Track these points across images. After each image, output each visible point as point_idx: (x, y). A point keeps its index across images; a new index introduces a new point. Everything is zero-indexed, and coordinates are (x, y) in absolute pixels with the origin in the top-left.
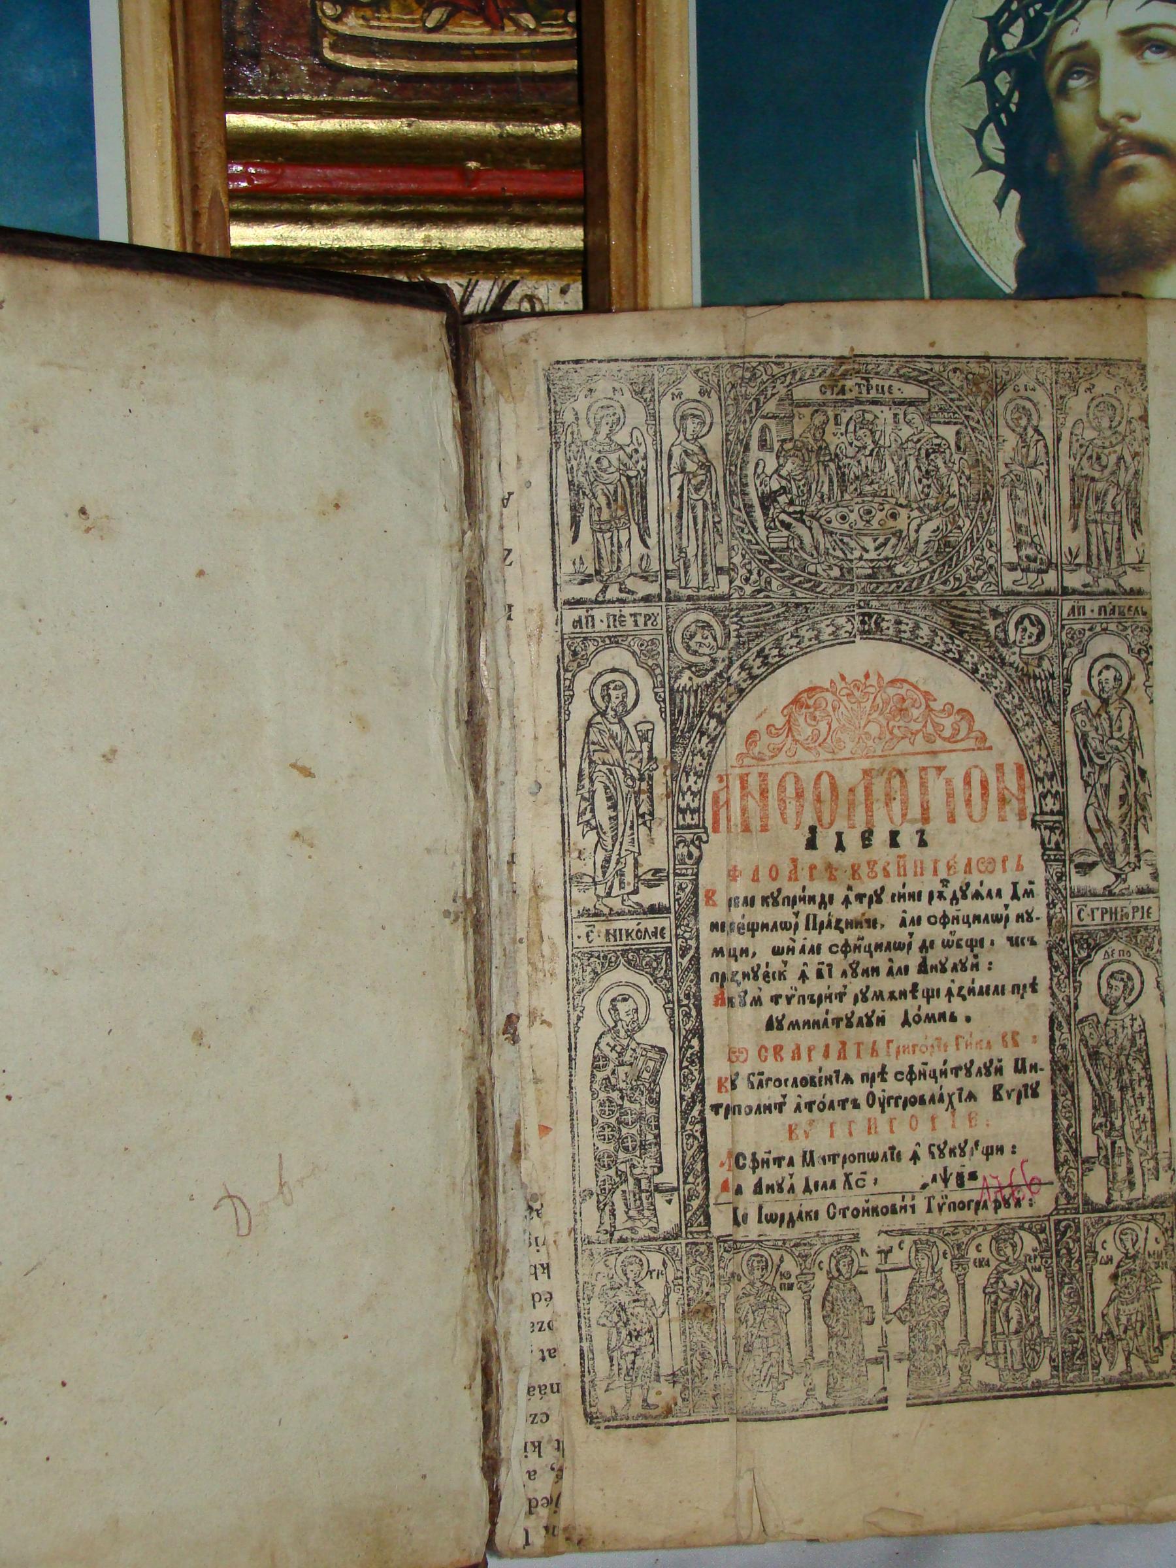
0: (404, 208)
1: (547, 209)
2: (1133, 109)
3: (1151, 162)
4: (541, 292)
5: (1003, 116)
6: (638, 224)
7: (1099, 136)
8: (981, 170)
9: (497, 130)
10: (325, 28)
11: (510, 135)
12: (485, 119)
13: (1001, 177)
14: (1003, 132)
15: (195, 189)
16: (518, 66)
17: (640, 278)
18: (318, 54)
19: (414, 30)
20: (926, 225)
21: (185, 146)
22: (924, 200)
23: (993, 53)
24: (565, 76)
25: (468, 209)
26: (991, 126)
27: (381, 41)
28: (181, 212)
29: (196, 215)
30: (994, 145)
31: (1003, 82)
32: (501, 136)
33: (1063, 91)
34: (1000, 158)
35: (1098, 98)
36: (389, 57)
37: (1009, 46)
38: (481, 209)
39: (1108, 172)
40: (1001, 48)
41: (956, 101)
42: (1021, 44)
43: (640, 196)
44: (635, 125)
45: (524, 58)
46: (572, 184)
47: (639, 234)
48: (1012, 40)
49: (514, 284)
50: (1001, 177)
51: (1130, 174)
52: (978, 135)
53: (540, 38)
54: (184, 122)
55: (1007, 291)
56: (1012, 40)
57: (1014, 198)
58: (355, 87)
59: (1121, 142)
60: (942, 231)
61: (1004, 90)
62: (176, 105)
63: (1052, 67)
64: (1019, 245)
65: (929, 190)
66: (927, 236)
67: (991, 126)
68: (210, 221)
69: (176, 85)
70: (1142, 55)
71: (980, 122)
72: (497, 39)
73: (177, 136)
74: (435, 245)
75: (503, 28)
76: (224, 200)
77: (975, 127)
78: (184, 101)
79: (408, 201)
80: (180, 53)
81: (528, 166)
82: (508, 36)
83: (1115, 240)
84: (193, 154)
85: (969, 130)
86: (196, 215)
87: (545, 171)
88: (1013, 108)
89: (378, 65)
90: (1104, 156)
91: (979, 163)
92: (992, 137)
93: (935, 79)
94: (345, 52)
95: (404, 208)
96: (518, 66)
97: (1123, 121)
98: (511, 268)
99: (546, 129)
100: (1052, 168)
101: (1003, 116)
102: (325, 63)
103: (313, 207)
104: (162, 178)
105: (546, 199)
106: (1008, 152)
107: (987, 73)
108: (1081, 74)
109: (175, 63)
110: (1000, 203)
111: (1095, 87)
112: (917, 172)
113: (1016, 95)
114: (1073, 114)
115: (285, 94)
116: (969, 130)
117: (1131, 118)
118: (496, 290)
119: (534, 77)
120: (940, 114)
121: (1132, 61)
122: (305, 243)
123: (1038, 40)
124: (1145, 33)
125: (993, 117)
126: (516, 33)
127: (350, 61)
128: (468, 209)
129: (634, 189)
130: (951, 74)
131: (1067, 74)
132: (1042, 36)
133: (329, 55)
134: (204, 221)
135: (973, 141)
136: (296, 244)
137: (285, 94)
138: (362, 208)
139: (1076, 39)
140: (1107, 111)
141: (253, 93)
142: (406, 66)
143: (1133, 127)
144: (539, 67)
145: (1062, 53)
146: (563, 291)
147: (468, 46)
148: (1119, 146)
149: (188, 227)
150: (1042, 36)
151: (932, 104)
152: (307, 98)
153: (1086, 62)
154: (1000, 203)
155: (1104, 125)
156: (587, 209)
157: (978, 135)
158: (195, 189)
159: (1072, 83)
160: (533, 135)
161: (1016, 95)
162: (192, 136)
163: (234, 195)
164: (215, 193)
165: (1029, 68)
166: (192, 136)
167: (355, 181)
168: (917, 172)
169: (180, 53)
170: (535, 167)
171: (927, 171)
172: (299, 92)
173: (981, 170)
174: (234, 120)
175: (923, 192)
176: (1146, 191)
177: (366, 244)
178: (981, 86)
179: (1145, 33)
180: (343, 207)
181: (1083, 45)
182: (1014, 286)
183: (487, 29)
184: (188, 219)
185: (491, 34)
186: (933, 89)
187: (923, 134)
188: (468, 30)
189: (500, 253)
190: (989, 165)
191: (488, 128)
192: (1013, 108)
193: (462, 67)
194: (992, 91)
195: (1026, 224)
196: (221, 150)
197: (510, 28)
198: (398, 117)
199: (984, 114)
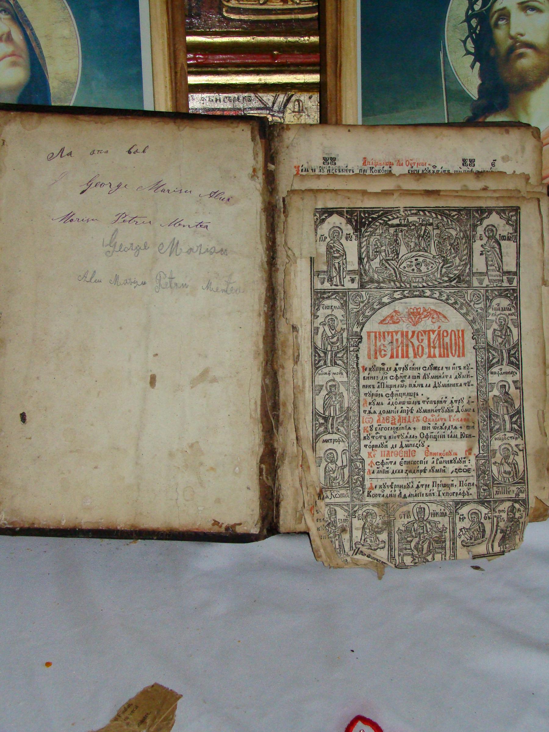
0: (251, 69)
1: (303, 68)
2: (522, 31)
3: (529, 51)
6: (338, 75)
7: (510, 42)
9: (285, 40)
10: (224, 5)
11: (289, 42)
12: (280, 36)
13: (473, 57)
14: (474, 41)
15: (175, 64)
16: (293, 16)
17: (338, 95)
18: (221, 14)
19: (256, 4)
20: (445, 75)
21: (172, 48)
22: (444, 66)
23: (470, 12)
24: (311, 19)
25: (274, 69)
26: (469, 39)
27: (243, 9)
28: (171, 72)
29: (176, 73)
30: (470, 46)
31: (474, 22)
32: (286, 42)
33: (496, 25)
34: (473, 51)
35: (509, 28)
36: (246, 14)
37: (476, 9)
39: (513, 56)
40: (473, 10)
41: (456, 30)
42: (481, 8)
43: (339, 65)
44: (337, 39)
45: (295, 14)
46: (314, 59)
47: (338, 78)
48: (477, 7)
49: (292, 95)
50: (473, 57)
51: (521, 56)
52: (464, 42)
53: (301, 6)
54: (171, 40)
55: (475, 99)
56: (477, 7)
57: (478, 65)
58: (235, 25)
59: (518, 44)
60: (450, 77)
62: (169, 34)
63: (492, 17)
64: (480, 82)
65: (446, 62)
66: (445, 79)
67: (469, 39)
68: (181, 75)
69: (169, 27)
70: (526, 12)
71: (465, 37)
72: (285, 7)
73: (169, 45)
74: (263, 82)
75: (287, 3)
76: (186, 67)
78: (171, 33)
79: (253, 67)
80: (170, 13)
81: (296, 52)
82: (290, 6)
83: (516, 80)
85: (461, 40)
86: (176, 73)
87: (302, 54)
88: (478, 32)
89: (242, 17)
90: (511, 49)
91: (465, 52)
92: (470, 43)
93: (449, 22)
94: (231, 13)
95: (251, 69)
96: (293, 16)
97: (519, 36)
98: (290, 90)
100: (492, 53)
101: (474, 35)
102: (224, 17)
103: (219, 69)
107: (468, 19)
108: (503, 19)
109: (168, 19)
110: (472, 67)
111: (508, 24)
112: (441, 55)
113: (479, 27)
114: (500, 34)
115: (210, 29)
116: (461, 40)
117: (522, 35)
118: (286, 98)
119: (299, 20)
120: (450, 35)
121: (522, 14)
122: (216, 82)
123: (487, 7)
124: (527, 4)
125: (470, 35)
126: (292, 5)
127: (233, 16)
128: (274, 69)
130: (454, 19)
131: (498, 19)
132: (489, 5)
133: (225, 14)
134: (179, 75)
135: (462, 44)
136: (213, 83)
137: (210, 29)
138: (236, 69)
139: (501, 6)
140: (513, 33)
141: (198, 29)
142: (253, 18)
143: (522, 38)
144: (301, 16)
145: (496, 12)
147: (275, 10)
148: (518, 45)
149: (173, 77)
150: (489, 5)
151: (447, 31)
152: (217, 30)
153: (505, 15)
154: (472, 67)
155: (512, 38)
157: (464, 42)
158: (175, 64)
159: (500, 23)
161: (479, 27)
162: (174, 45)
163: (190, 66)
164: (182, 64)
165: (483, 17)
166: (174, 45)
167: (234, 59)
168: (441, 55)
169: (170, 13)
170: (298, 53)
171: (445, 55)
172: (214, 27)
174: (189, 39)
175: (444, 63)
176: (528, 62)
177: (238, 82)
178: (466, 24)
179: (527, 4)
180: (230, 69)
181: (504, 8)
182: (477, 97)
183: (282, 3)
185: (283, 5)
186: (448, 25)
187: (444, 42)
188: (275, 4)
189: (286, 84)
190: (468, 53)
191: (282, 39)
192: (478, 32)
193: (273, 17)
194: (470, 26)
195: (482, 74)
196: (185, 50)
197: (290, 3)
198: (249, 36)
199: (467, 34)
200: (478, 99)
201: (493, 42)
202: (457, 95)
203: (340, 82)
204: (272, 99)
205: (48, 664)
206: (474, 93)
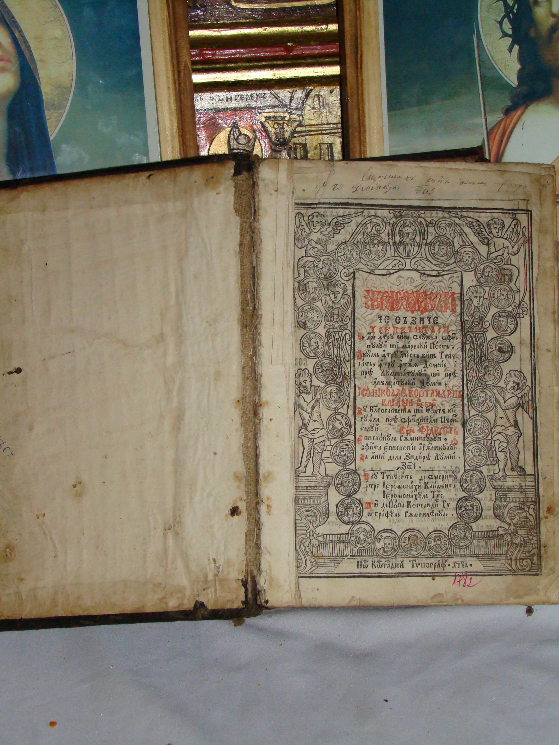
0: (264, 63)
1: (321, 60)
4: (322, 93)
5: (511, 15)
8: (502, 37)
9: (301, 30)
11: (305, 31)
13: (511, 40)
14: (511, 22)
15: (178, 62)
20: (479, 61)
21: (174, 45)
22: (478, 51)
26: (506, 19)
28: (174, 71)
29: (179, 72)
30: (507, 27)
32: (302, 32)
34: (510, 32)
38: (295, 62)
41: (491, 10)
46: (333, 49)
50: (511, 40)
54: (173, 36)
55: (514, 86)
57: (516, 48)
60: (486, 63)
61: (511, 4)
62: (170, 30)
64: (519, 67)
65: (481, 47)
66: (480, 65)
67: (506, 19)
68: (184, 74)
71: (501, 17)
73: (170, 43)
74: (277, 77)
76: (189, 66)
77: (499, 20)
79: (266, 61)
84: (177, 49)
86: (179, 72)
87: (319, 45)
88: (515, 11)
91: (501, 34)
92: (506, 23)
95: (264, 63)
99: (319, 27)
100: (532, 34)
101: (511, 15)
103: (228, 65)
104: (166, 59)
105: (320, 56)
106: (513, 29)
110: (510, 50)
113: (516, 6)
116: (497, 22)
118: (304, 94)
120: (484, 15)
122: (226, 80)
125: (506, 15)
129: (357, 53)
135: (498, 25)
136: (222, 80)
138: (248, 64)
146: (331, 92)
149: (176, 77)
151: (481, 11)
154: (510, 50)
156: (339, 59)
157: (501, 23)
158: (178, 62)
160: (314, 31)
161: (516, 6)
162: (176, 42)
163: (194, 63)
164: (186, 62)
166: (176, 42)
167: (244, 54)
170: (315, 43)
171: (479, 39)
173: (502, 37)
174: (193, 33)
175: (478, 47)
177: (250, 79)
180: (239, 64)
182: (517, 84)
184: (176, 73)
187: (477, 24)
189: (304, 79)
190: (505, 35)
192: (515, 11)
195: (521, 58)
196: (188, 46)
200: (518, 85)
201: (532, 22)
202: (493, 82)
203: (362, 75)
204: (288, 95)
205: (53, 724)
206: (513, 81)
